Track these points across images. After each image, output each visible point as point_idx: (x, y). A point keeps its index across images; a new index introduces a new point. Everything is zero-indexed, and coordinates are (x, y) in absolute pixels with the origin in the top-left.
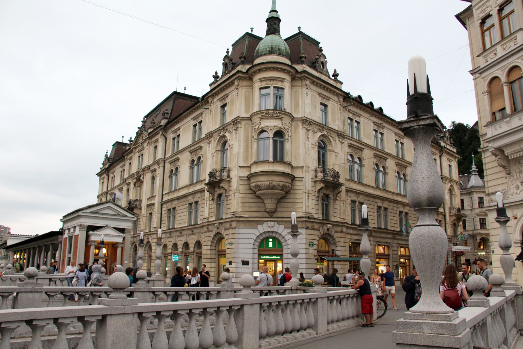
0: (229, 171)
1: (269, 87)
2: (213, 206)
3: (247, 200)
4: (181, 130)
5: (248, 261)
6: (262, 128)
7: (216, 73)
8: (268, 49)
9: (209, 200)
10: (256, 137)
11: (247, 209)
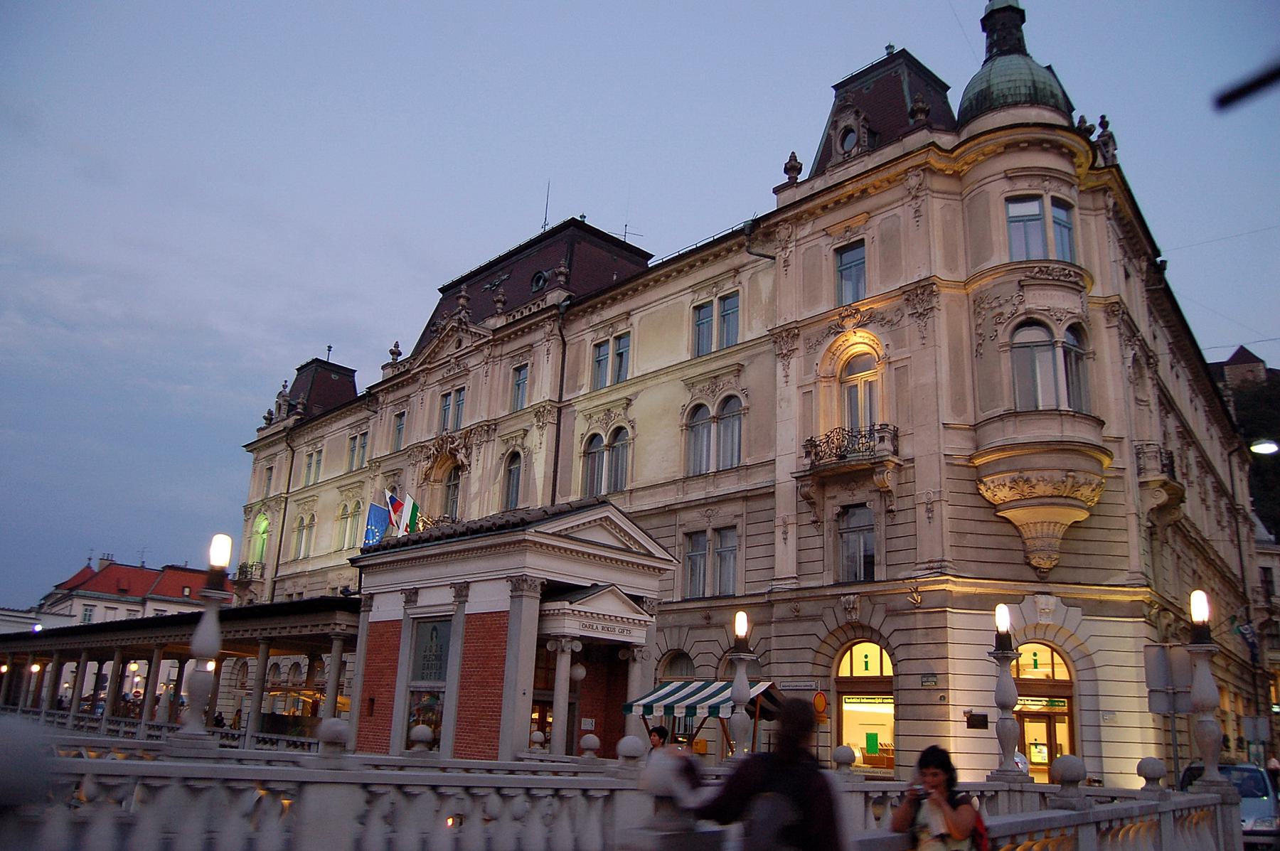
0: (895, 437)
2: (818, 542)
3: (968, 526)
4: (635, 319)
5: (986, 716)
6: (1027, 312)
7: (793, 157)
8: (1023, 91)
9: (799, 526)
10: (1004, 338)
11: (971, 554)
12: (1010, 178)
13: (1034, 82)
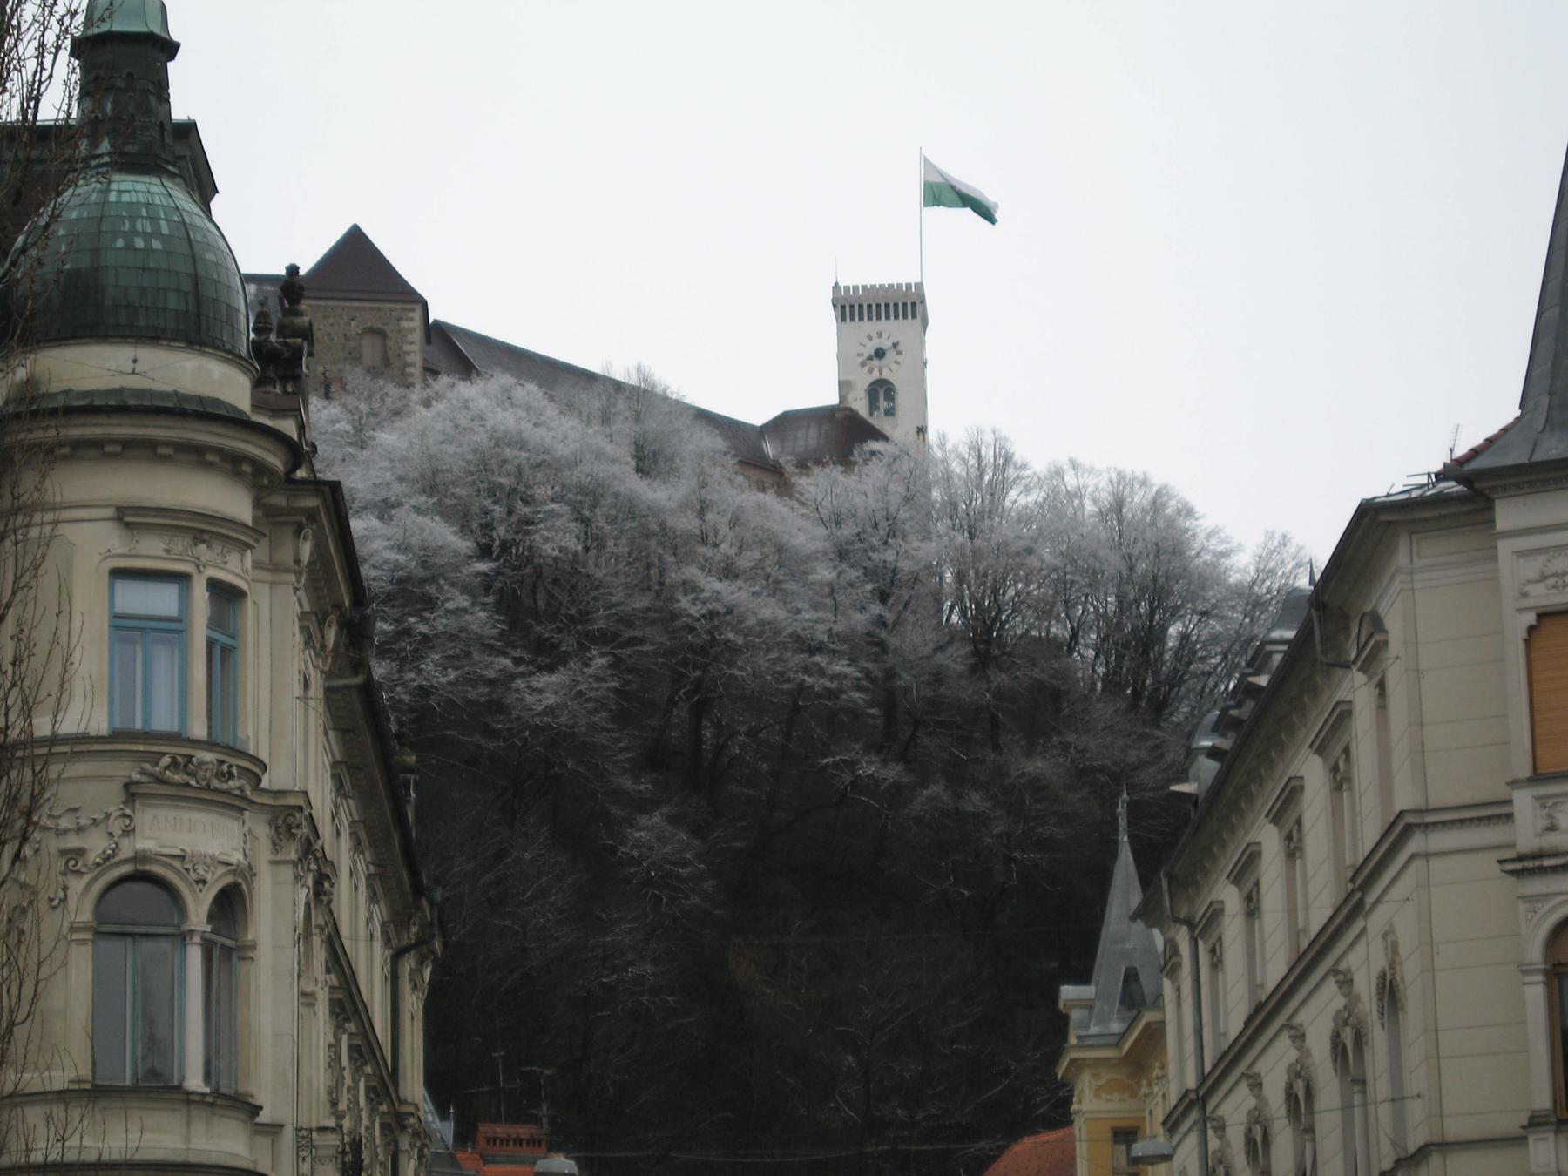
1: (182, 579)
6: (140, 857)
8: (173, 302)
12: (127, 525)
13: (196, 280)
